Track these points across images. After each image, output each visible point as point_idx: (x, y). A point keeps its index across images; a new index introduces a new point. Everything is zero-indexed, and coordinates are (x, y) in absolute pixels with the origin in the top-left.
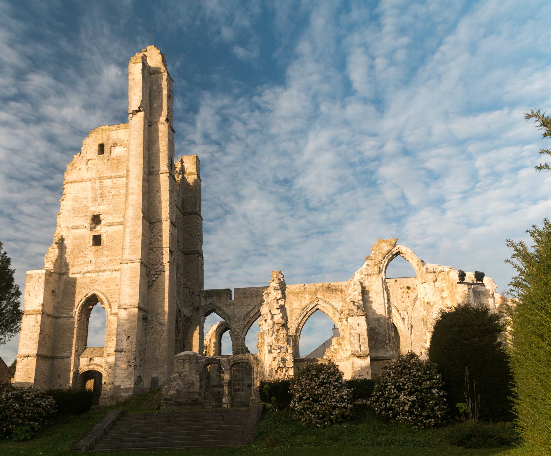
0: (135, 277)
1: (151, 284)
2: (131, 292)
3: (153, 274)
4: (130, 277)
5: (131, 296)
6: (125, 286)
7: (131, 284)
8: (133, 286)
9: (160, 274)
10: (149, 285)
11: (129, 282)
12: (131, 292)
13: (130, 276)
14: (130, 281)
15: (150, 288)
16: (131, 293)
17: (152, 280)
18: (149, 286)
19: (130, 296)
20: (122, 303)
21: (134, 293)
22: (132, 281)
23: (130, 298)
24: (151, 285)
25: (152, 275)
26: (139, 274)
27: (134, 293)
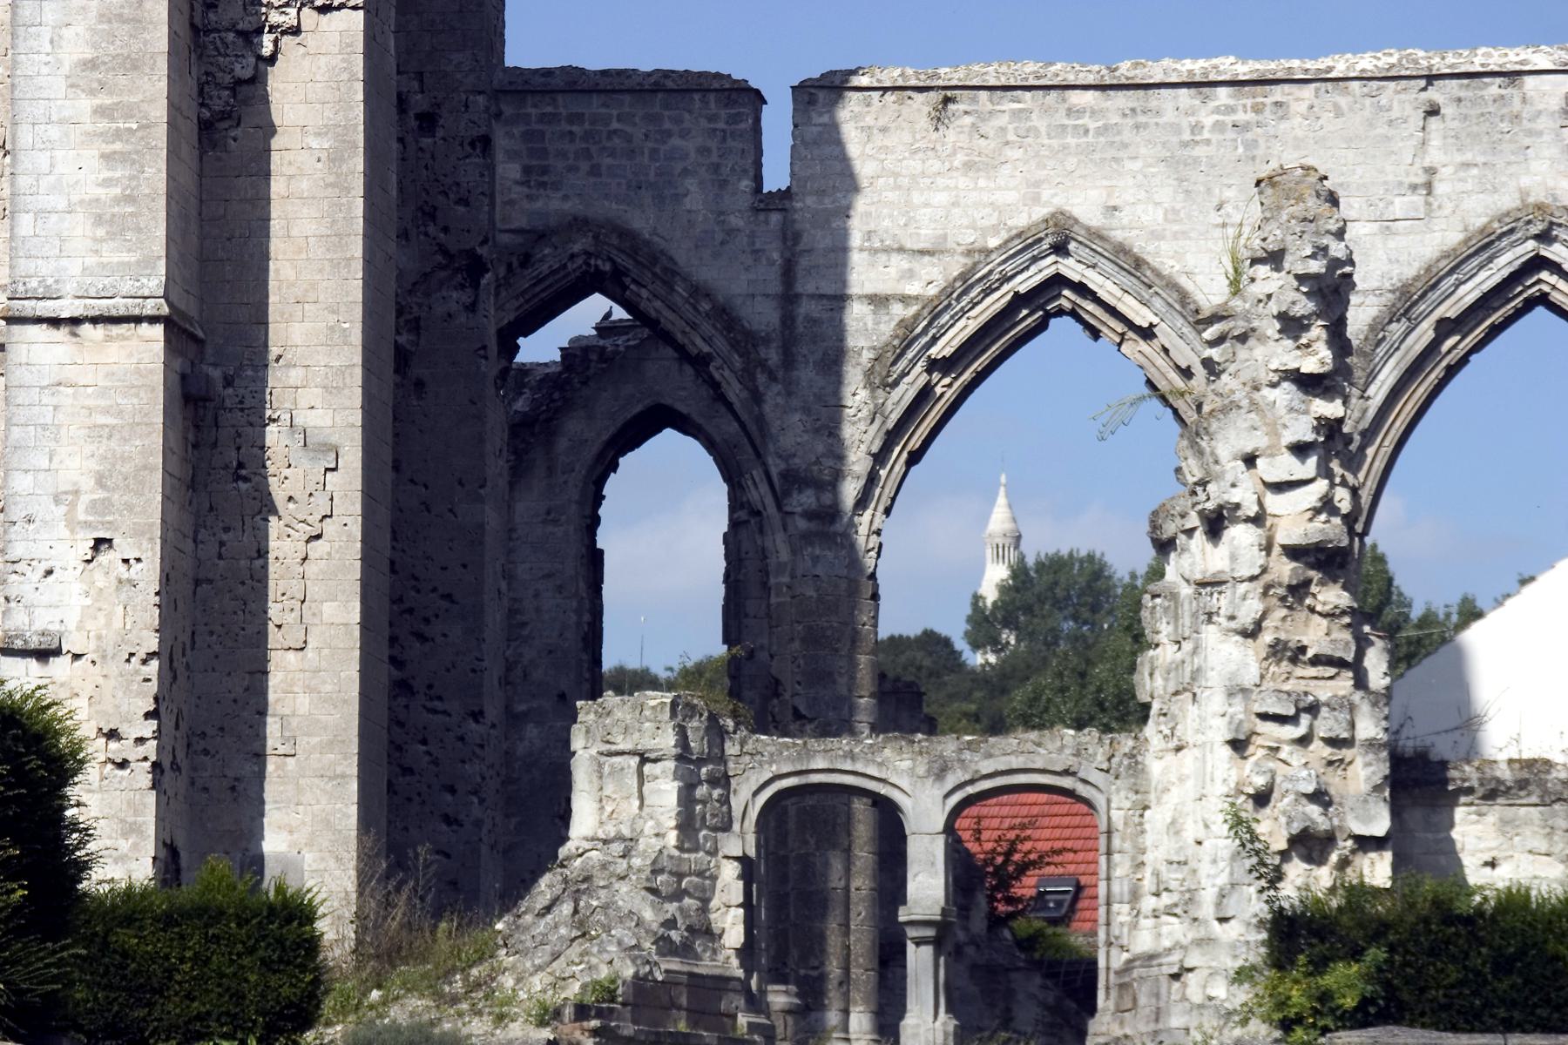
0: (132, 64)
1: (217, 105)
2: (107, 183)
3: (232, 28)
4: (91, 65)
5: (111, 224)
6: (54, 132)
7: (103, 125)
8: (118, 135)
9: (296, 31)
10: (206, 114)
11: (86, 104)
12: (107, 183)
13: (89, 54)
14: (92, 93)
15: (214, 146)
16: (101, 192)
17: (227, 79)
18: (205, 127)
19: (99, 220)
20: (38, 270)
21: (130, 199)
22: (105, 100)
23: (101, 232)
24: (225, 115)
25: (231, 36)
26: (163, 45)
27: (130, 199)
